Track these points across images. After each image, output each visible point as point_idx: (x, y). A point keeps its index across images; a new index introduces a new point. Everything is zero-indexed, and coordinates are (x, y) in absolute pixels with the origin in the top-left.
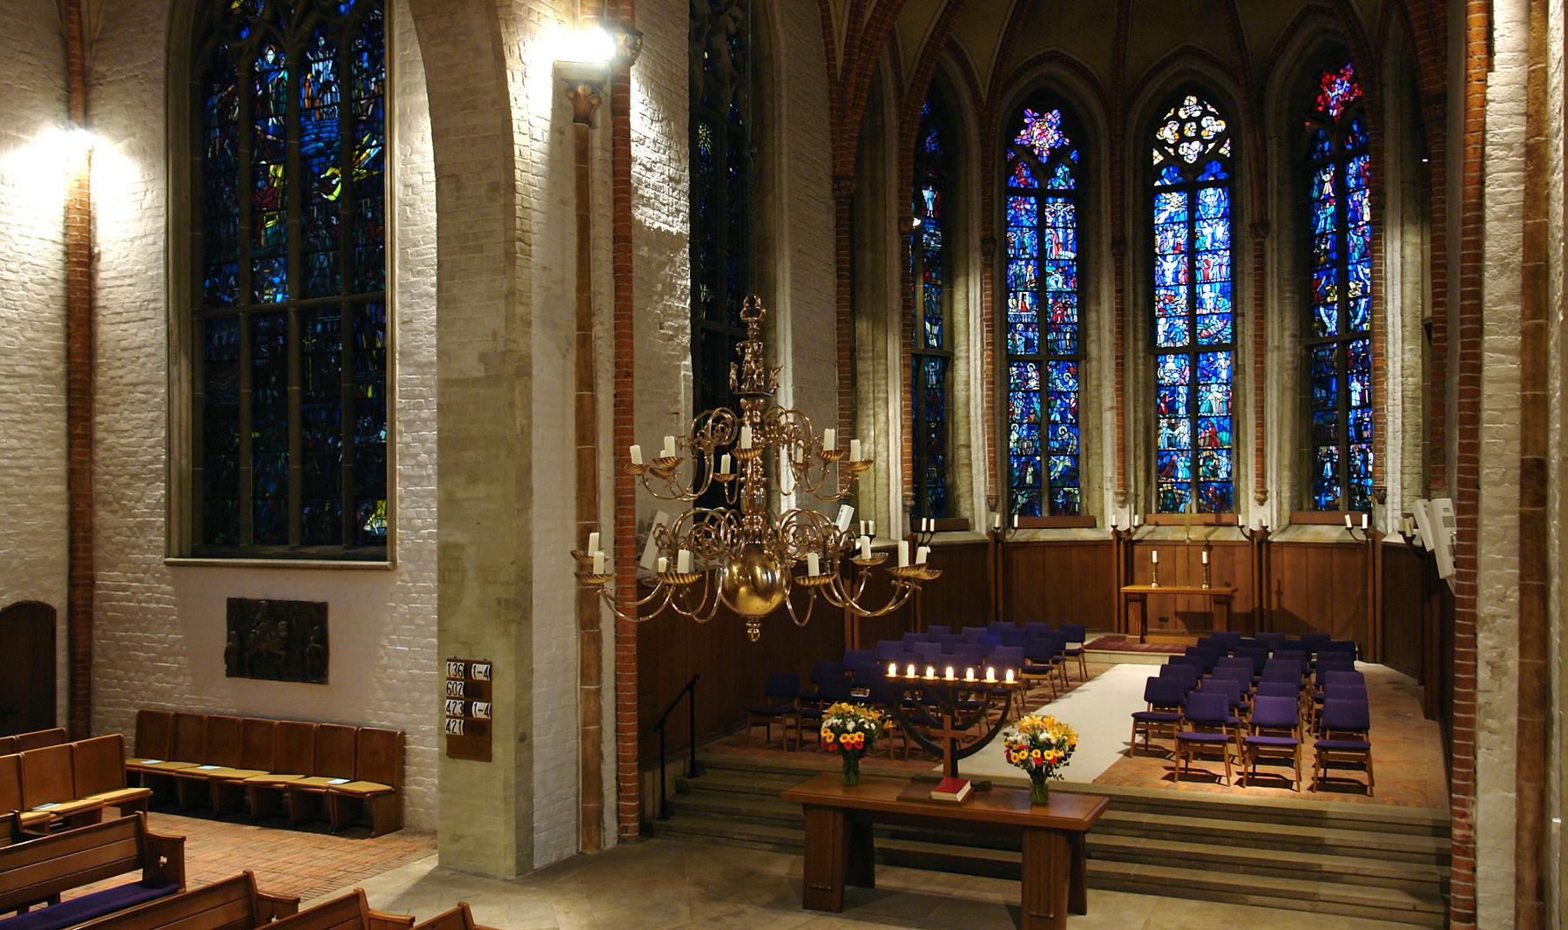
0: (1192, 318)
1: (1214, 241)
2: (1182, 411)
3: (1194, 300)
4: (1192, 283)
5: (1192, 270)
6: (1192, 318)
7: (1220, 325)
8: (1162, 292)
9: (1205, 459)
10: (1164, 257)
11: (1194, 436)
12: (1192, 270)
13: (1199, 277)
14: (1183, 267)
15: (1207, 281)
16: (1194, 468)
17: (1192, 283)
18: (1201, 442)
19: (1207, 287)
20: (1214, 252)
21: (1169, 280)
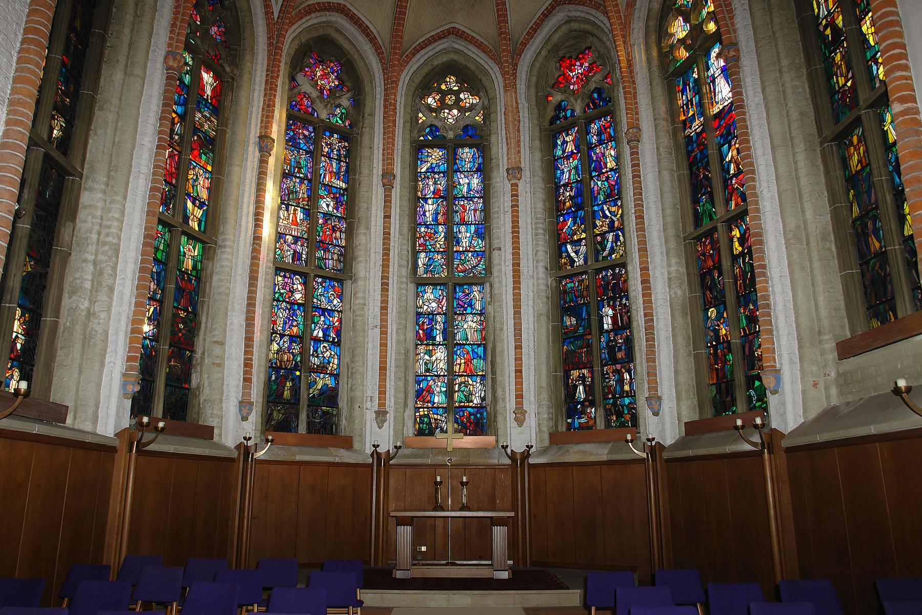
0: (449, 254)
1: (469, 190)
2: (439, 338)
3: (452, 239)
4: (449, 223)
5: (449, 214)
6: (449, 254)
7: (474, 262)
8: (423, 229)
9: (460, 384)
10: (426, 200)
11: (450, 363)
12: (449, 214)
13: (457, 219)
14: (442, 210)
15: (463, 222)
16: (449, 393)
17: (449, 223)
18: (457, 368)
19: (463, 228)
20: (470, 199)
21: (429, 218)
